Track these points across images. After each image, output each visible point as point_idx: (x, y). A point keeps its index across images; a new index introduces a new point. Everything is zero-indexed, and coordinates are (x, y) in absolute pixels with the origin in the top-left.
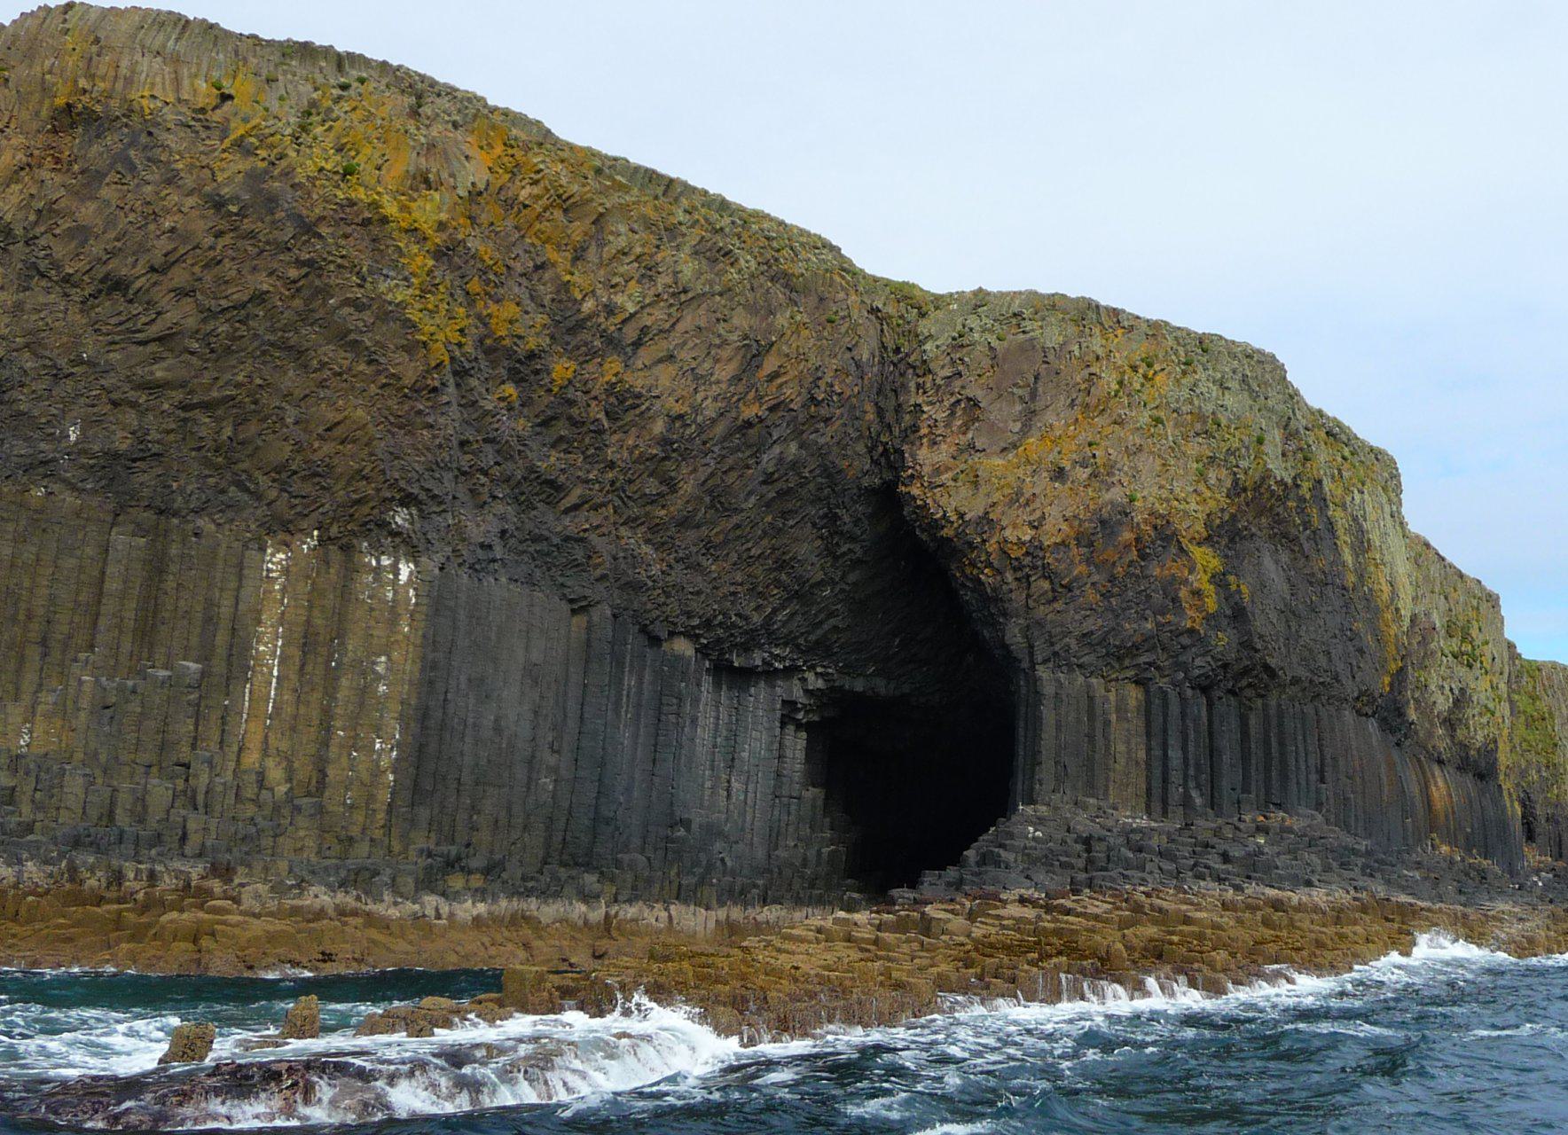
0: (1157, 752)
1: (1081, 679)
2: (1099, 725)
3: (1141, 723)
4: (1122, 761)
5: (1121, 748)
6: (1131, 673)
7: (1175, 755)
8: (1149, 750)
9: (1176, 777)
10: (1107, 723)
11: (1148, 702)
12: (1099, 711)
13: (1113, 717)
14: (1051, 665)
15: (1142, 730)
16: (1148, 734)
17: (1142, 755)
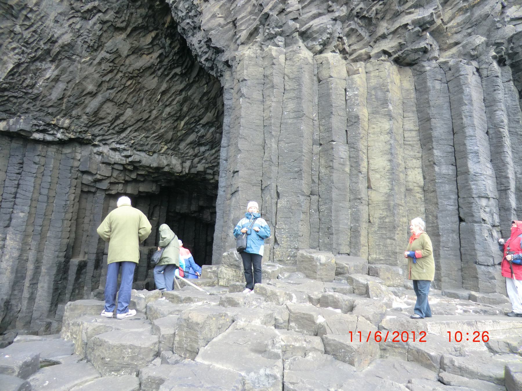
0: (445, 169)
1: (305, 54)
2: (337, 122)
3: (411, 124)
4: (382, 185)
5: (380, 162)
6: (388, 45)
7: (481, 168)
8: (428, 166)
9: (486, 210)
10: (353, 121)
11: (421, 89)
12: (338, 100)
13: (364, 112)
14: (259, 38)
15: (413, 136)
16: (426, 141)
17: (416, 176)
